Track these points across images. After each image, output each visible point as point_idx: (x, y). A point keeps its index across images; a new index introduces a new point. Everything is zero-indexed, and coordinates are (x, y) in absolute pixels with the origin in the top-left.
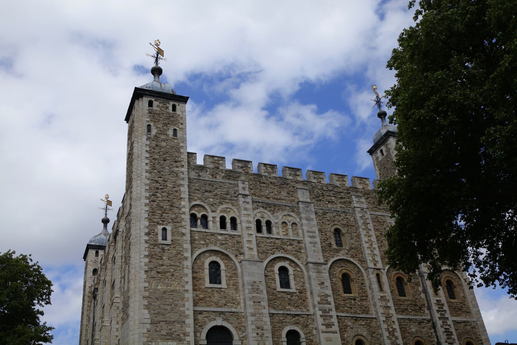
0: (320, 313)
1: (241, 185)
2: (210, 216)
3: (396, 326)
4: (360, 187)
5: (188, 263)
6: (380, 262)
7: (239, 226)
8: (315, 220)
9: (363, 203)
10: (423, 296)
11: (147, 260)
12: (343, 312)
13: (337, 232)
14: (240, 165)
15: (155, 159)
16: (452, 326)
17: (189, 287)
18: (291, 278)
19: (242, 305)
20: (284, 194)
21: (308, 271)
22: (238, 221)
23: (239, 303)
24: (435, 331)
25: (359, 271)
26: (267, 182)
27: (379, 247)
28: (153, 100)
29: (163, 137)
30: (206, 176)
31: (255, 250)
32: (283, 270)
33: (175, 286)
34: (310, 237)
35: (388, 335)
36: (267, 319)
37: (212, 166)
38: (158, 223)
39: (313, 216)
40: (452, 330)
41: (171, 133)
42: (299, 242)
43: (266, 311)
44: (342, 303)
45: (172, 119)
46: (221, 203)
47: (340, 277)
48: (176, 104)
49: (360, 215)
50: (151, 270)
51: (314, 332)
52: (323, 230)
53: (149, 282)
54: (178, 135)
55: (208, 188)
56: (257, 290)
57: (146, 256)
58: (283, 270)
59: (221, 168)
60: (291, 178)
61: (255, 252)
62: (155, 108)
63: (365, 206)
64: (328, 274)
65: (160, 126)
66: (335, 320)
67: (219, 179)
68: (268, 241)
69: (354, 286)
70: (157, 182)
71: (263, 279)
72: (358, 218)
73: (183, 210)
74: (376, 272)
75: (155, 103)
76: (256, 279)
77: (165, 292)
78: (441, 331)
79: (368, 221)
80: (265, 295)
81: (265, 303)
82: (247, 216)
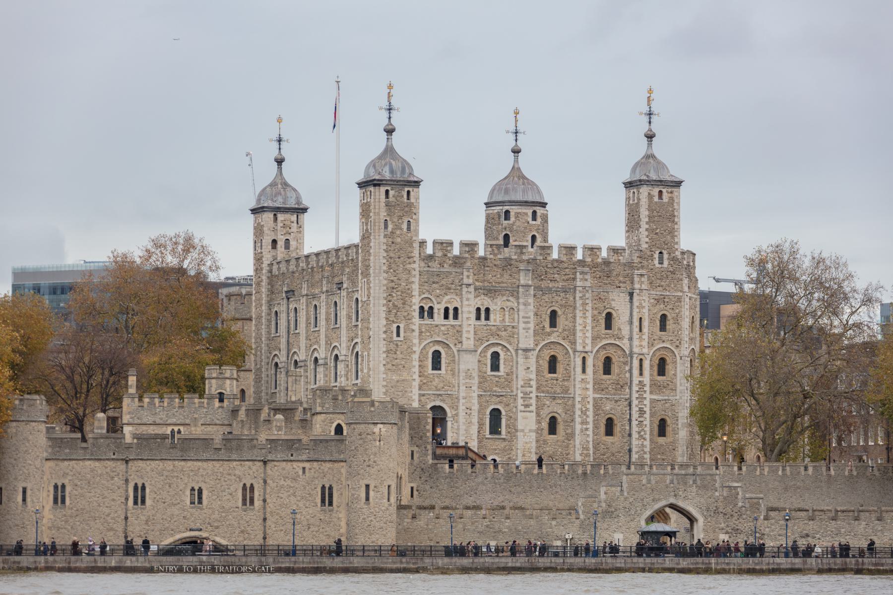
0: (522, 395)
1: (466, 273)
2: (436, 307)
3: (590, 406)
4: (589, 260)
5: (416, 357)
6: (590, 345)
7: (460, 316)
8: (532, 304)
9: (586, 280)
10: (628, 375)
11: (385, 355)
12: (543, 392)
13: (554, 314)
14: (467, 249)
15: (391, 258)
16: (648, 406)
17: (416, 376)
18: (502, 362)
19: (457, 388)
20: (506, 276)
21: (517, 356)
22: (460, 312)
23: (454, 386)
24: (630, 409)
25: (567, 353)
26: (491, 265)
27: (593, 328)
28: (389, 188)
29: (398, 232)
30: (435, 266)
31: (472, 339)
32: (495, 356)
33: (405, 376)
34: (525, 323)
35: (580, 413)
36: (475, 401)
37: (439, 254)
38: (393, 321)
39: (531, 300)
40: (647, 409)
41: (405, 226)
42: (513, 327)
43: (475, 395)
44: (544, 383)
45: (406, 209)
46: (446, 294)
47: (548, 359)
48: (411, 189)
49: (581, 295)
50: (388, 363)
51: (514, 410)
52: (539, 313)
53: (386, 374)
54: (412, 228)
55: (436, 279)
56: (470, 377)
57: (384, 352)
58: (495, 356)
59: (449, 255)
60: (516, 257)
61: (472, 342)
62: (391, 198)
63: (588, 284)
64: (535, 360)
65: (395, 220)
66: (533, 401)
67: (447, 268)
68: (485, 328)
69: (560, 368)
70: (392, 281)
71: (476, 368)
72: (577, 298)
73: (414, 307)
74: (583, 355)
75: (391, 193)
76: (470, 368)
77: (398, 381)
78: (635, 409)
79: (587, 301)
80: (476, 381)
81: (475, 388)
82: (469, 304)
